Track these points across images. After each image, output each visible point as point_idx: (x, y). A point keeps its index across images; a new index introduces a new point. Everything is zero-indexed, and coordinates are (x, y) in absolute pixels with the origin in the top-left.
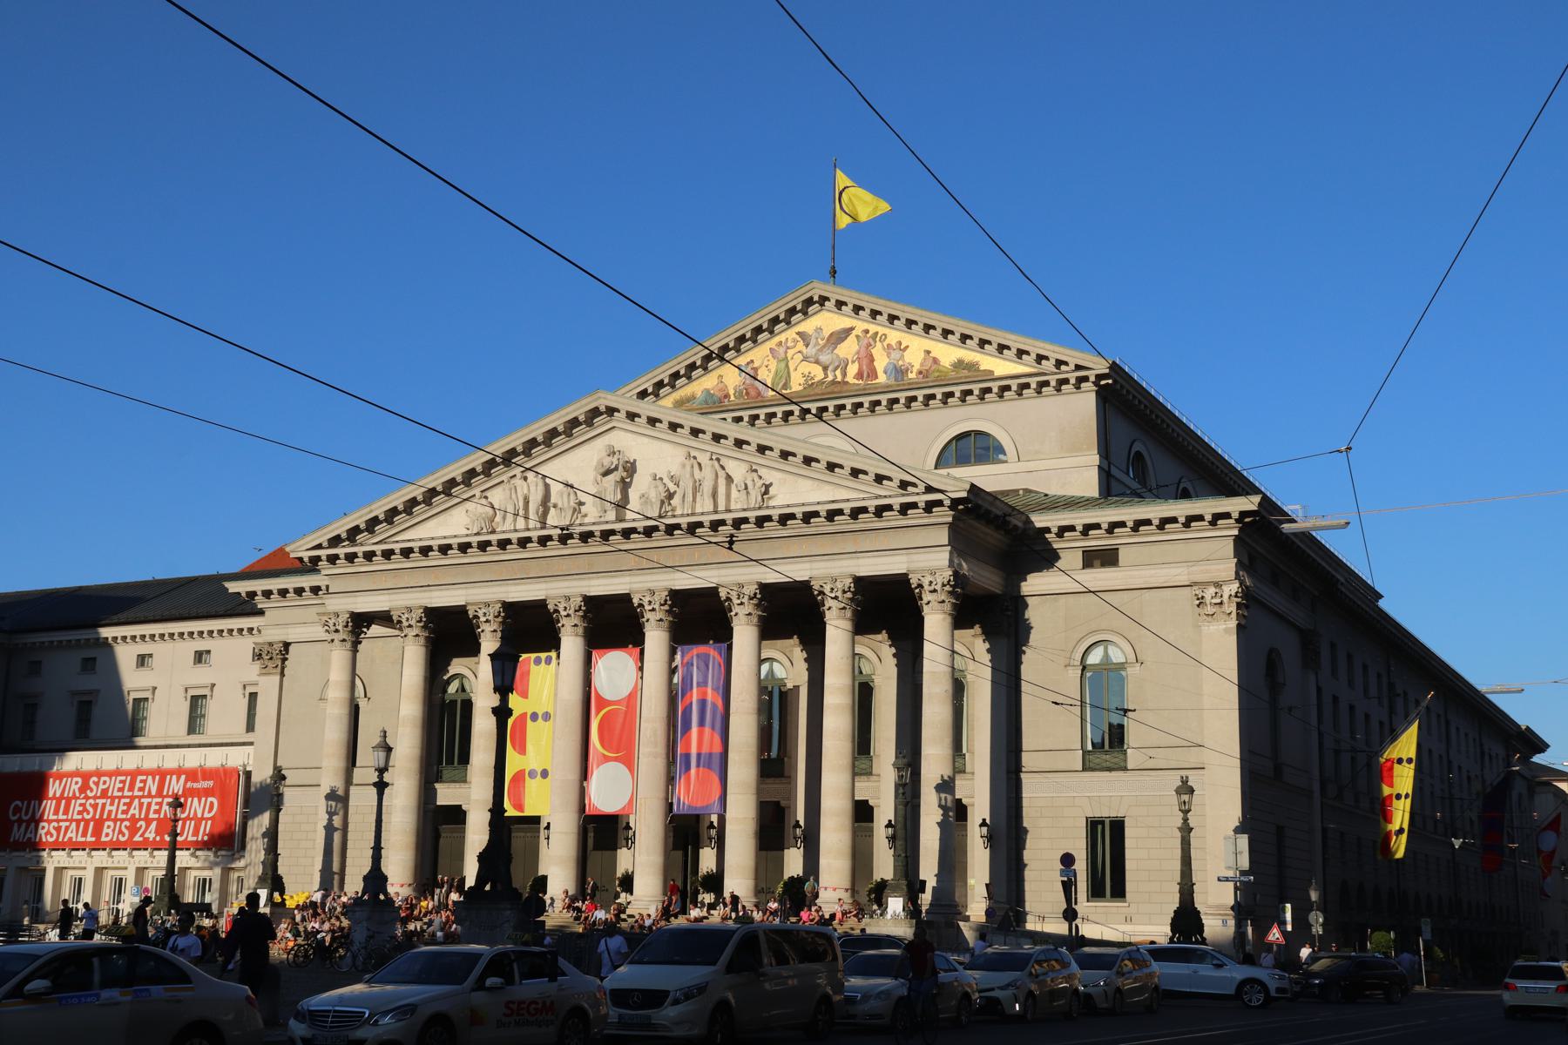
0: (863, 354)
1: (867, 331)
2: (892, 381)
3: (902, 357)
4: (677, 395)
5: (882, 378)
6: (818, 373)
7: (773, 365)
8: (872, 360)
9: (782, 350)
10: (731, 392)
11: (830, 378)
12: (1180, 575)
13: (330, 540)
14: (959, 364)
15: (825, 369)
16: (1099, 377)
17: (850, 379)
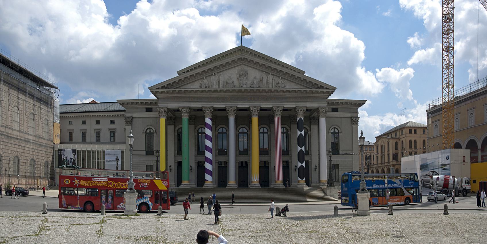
12: (349, 115)
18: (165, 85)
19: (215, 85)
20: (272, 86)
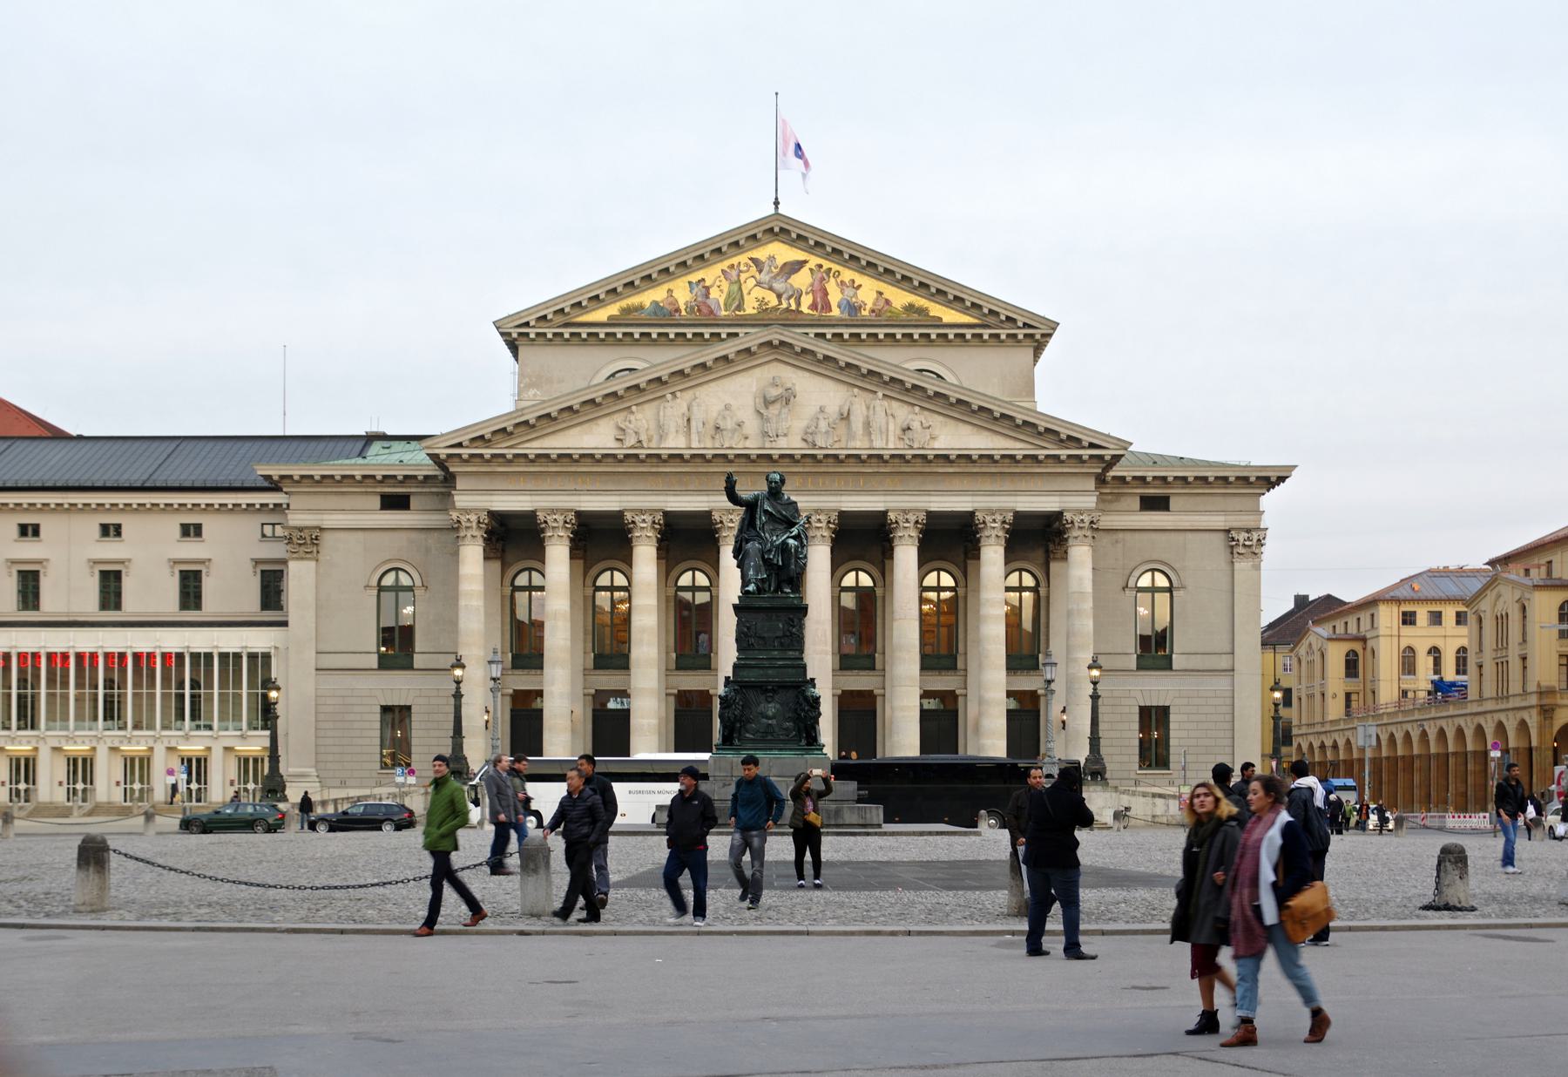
1: (820, 266)
2: (846, 316)
3: (855, 295)
5: (836, 312)
7: (725, 285)
8: (826, 294)
9: (734, 273)
10: (683, 307)
11: (785, 305)
12: (1219, 521)
13: (473, 440)
14: (910, 308)
15: (779, 296)
16: (1043, 335)
17: (805, 309)
18: (487, 432)
19: (671, 437)
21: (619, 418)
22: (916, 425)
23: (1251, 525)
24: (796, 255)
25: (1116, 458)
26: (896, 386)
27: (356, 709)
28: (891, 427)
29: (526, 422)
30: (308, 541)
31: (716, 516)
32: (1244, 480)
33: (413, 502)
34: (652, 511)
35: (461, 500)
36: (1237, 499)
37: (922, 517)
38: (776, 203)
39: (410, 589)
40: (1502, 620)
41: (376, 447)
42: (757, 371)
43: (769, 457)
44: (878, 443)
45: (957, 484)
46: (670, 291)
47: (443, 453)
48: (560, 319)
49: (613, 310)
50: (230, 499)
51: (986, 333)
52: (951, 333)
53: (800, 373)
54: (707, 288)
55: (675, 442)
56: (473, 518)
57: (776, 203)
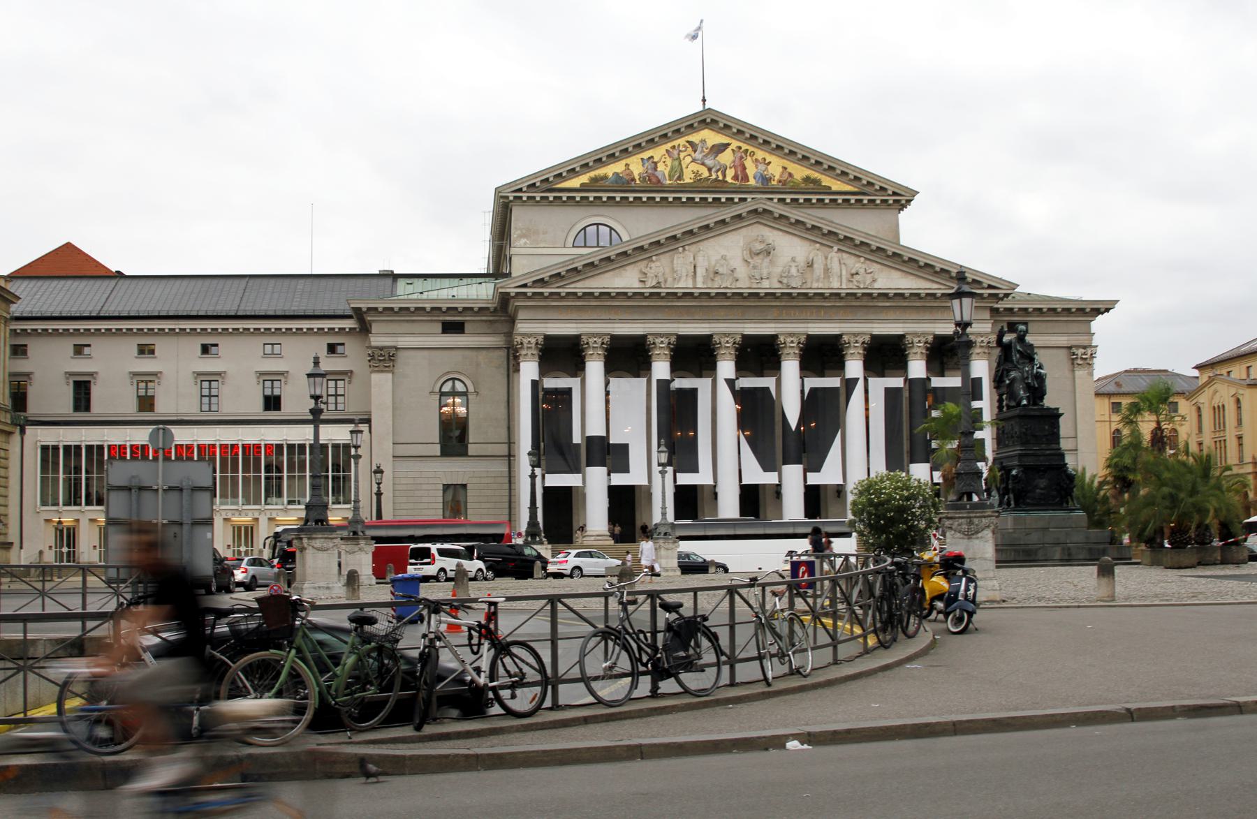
0: (737, 163)
1: (740, 148)
2: (759, 185)
4: (592, 174)
5: (752, 182)
6: (706, 174)
7: (669, 161)
8: (744, 168)
9: (675, 152)
10: (637, 178)
11: (714, 176)
12: (1063, 340)
13: (534, 282)
14: (807, 179)
15: (710, 170)
17: (729, 179)
18: (546, 276)
20: (837, 284)
21: (642, 265)
22: (862, 271)
23: (1086, 343)
24: (720, 139)
25: (1007, 295)
26: (851, 244)
27: (424, 487)
28: (844, 273)
29: (576, 269)
30: (384, 359)
31: (716, 339)
32: (1081, 311)
33: (467, 327)
34: (667, 335)
35: (521, 327)
36: (1049, 324)
37: (867, 338)
38: (704, 100)
39: (464, 394)
40: (1219, 410)
41: (401, 283)
42: (744, 231)
43: (757, 294)
44: (836, 284)
45: (891, 315)
46: (627, 165)
47: (513, 291)
48: (546, 186)
49: (584, 179)
50: (305, 325)
51: (865, 199)
52: (840, 199)
53: (776, 232)
54: (656, 163)
55: (684, 284)
56: (533, 341)
57: (704, 100)
